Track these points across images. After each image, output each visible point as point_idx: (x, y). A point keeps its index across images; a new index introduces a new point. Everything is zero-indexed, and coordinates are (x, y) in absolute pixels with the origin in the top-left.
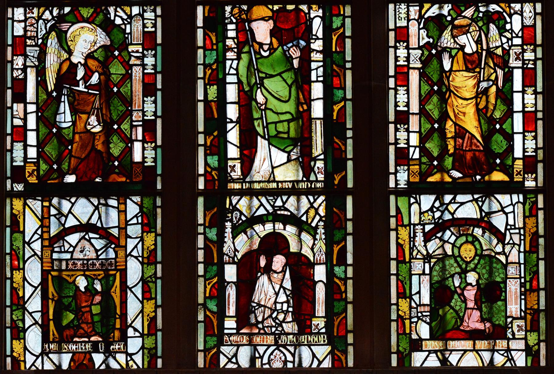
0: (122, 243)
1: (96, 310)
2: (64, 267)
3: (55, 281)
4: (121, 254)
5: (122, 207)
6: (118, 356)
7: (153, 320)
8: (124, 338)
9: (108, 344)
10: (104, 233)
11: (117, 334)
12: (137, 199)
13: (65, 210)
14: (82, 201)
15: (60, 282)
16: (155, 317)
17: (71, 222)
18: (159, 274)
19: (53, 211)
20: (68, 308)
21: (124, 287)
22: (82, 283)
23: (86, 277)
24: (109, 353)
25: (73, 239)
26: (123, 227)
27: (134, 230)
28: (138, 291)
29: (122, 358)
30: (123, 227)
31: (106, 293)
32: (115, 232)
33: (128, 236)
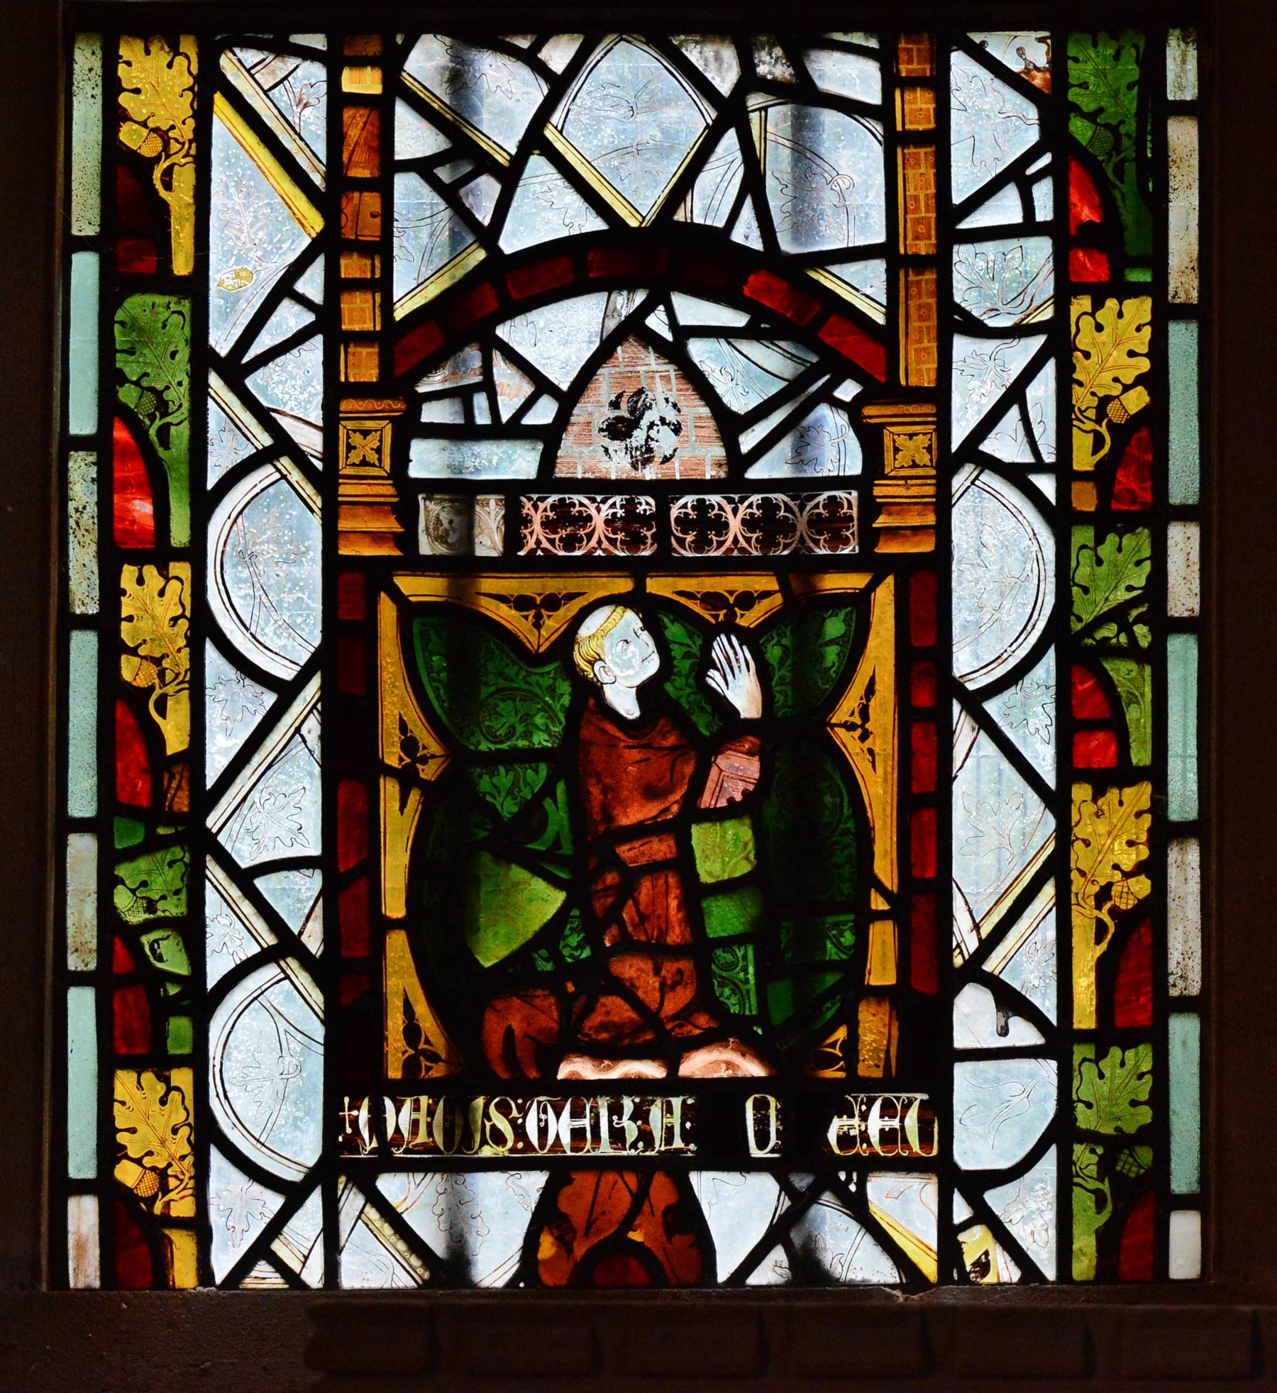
0: (917, 369)
1: (721, 852)
2: (489, 542)
3: (422, 643)
4: (909, 446)
5: (915, 109)
6: (883, 1192)
7: (1136, 933)
8: (927, 1063)
9: (808, 1099)
10: (781, 294)
11: (874, 1029)
12: (1026, 50)
13: (501, 128)
14: (626, 64)
15: (460, 648)
16: (1152, 913)
17: (544, 214)
18: (1184, 595)
19: (414, 137)
20: (517, 842)
21: (932, 696)
22: (621, 657)
23: (654, 614)
24: (817, 1172)
25: (558, 335)
26: (924, 247)
27: (1003, 275)
28: (1031, 716)
29: (906, 1205)
30: (924, 247)
31: (797, 735)
32: (864, 287)
33: (956, 321)
